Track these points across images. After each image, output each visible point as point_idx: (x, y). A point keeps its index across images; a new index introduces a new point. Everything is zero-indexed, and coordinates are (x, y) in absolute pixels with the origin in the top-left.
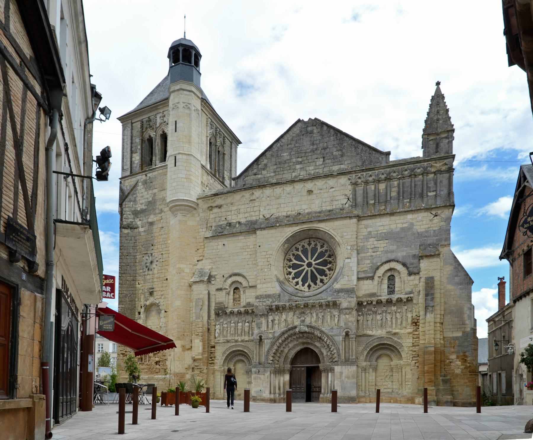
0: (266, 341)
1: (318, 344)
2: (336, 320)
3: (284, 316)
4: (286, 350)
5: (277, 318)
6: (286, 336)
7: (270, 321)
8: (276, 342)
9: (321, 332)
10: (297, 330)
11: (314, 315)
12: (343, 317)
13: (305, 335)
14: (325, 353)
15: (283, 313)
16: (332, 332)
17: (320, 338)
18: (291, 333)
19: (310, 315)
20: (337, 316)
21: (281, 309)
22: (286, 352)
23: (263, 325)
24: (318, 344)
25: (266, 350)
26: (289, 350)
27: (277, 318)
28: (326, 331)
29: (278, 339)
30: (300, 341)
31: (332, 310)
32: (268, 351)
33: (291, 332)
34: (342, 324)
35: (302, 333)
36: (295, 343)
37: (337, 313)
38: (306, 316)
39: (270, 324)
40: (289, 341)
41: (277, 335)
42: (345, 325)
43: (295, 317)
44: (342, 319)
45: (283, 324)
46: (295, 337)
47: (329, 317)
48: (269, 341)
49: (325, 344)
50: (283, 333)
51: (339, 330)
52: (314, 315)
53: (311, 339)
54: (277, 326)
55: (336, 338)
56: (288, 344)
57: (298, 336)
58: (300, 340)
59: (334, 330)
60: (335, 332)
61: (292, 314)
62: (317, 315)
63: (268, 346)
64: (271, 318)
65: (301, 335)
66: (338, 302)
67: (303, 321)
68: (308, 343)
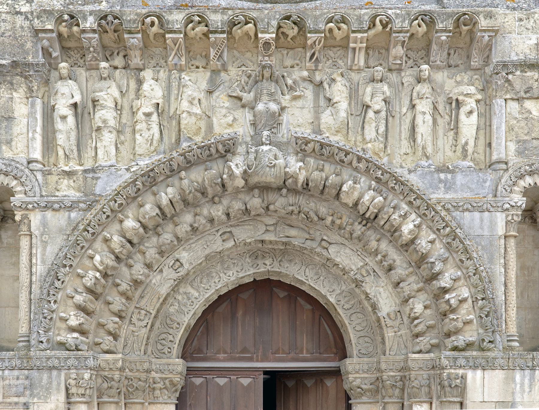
0: (36, 219)
1: (346, 257)
2: (469, 125)
3: (153, 89)
4: (162, 282)
5: (108, 93)
6: (167, 194)
7: (63, 107)
8: (103, 225)
9: (387, 181)
10: (237, 165)
11: (339, 91)
12: (505, 110)
13: (280, 202)
14: (386, 303)
15: (147, 74)
16: (449, 187)
17: (369, 220)
18: (191, 180)
19: (309, 93)
20: (471, 104)
21: (135, 40)
22: (164, 290)
23: (20, 127)
24: (346, 257)
25: (40, 269)
26: (181, 281)
27: (108, 93)
28: (414, 180)
29: (115, 214)
30: (246, 234)
31: (440, 76)
32: (54, 276)
33: (197, 176)
34: (505, 148)
35: (265, 188)
36: (218, 245)
37: (472, 89)
38: (286, 100)
39: (66, 129)
40: (183, 229)
41: (106, 186)
42: (520, 153)
43: (221, 100)
44: (500, 125)
45: (148, 132)
46: (218, 212)
47: (424, 106)
48: (58, 220)
49: (395, 256)
50: (150, 180)
51: (490, 177)
52: (339, 91)
53: (309, 221)
54: (108, 138)
55: (472, 221)
56: (173, 249)
57: (237, 206)
58: (246, 234)
59: (460, 179)
60: (466, 186)
61: (204, 85)
62: (354, 93)
63: (52, 250)
64: (67, 93)
65: (256, 202)
66: (483, 23)
67: (274, 120)
68: (285, 251)
